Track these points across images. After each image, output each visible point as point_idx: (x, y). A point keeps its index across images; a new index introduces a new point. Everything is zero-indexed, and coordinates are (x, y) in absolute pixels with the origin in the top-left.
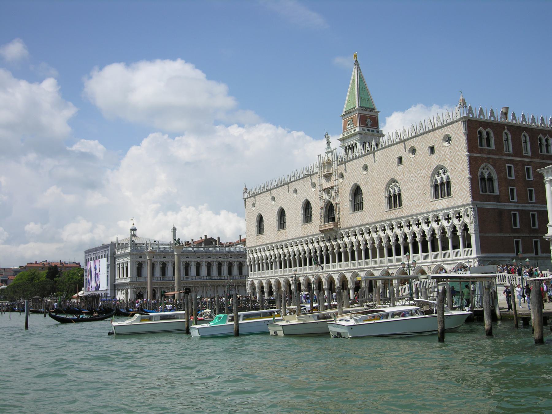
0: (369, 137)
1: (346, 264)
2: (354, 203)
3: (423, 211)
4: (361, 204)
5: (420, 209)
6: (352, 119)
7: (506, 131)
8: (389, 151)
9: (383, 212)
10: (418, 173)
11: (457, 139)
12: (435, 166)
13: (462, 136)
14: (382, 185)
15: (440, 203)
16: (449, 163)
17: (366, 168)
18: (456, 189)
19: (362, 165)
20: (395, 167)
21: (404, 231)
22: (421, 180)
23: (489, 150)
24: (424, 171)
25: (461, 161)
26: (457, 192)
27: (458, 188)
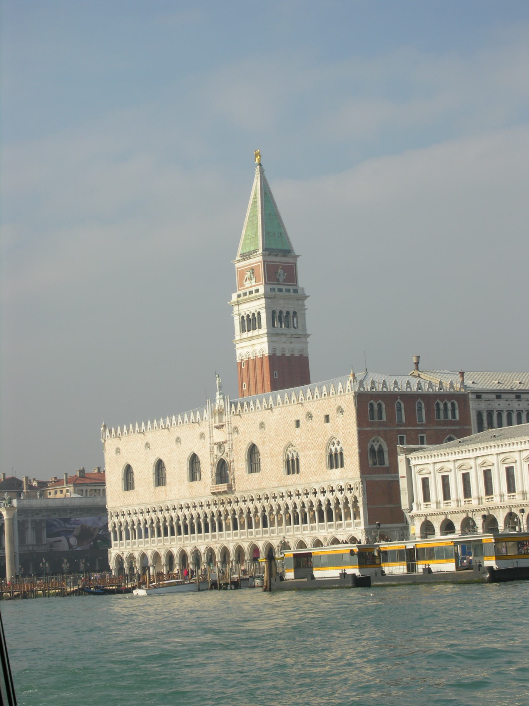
0: (282, 302)
1: (243, 532)
2: (251, 463)
3: (318, 480)
4: (259, 464)
5: (316, 478)
6: (253, 269)
7: (399, 400)
9: (281, 478)
10: (315, 440)
11: (348, 413)
12: (330, 437)
14: (280, 447)
15: (334, 473)
17: (262, 425)
23: (380, 422)
24: (320, 439)
25: (352, 435)
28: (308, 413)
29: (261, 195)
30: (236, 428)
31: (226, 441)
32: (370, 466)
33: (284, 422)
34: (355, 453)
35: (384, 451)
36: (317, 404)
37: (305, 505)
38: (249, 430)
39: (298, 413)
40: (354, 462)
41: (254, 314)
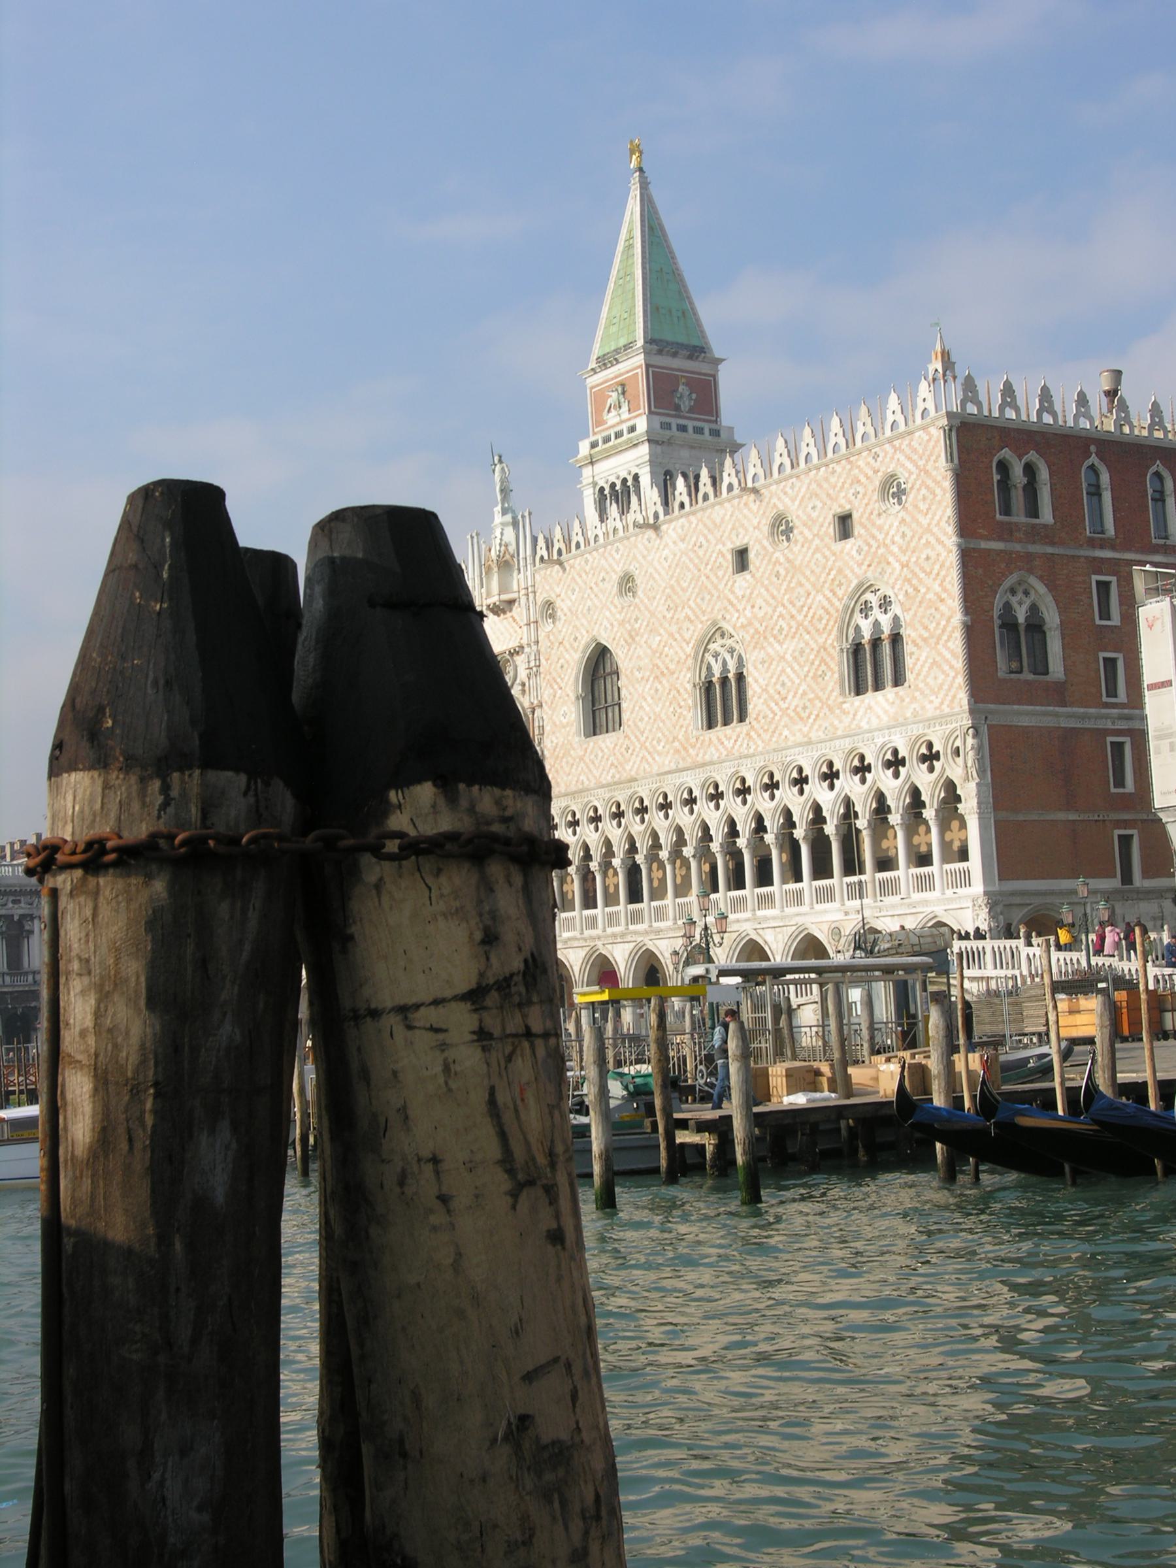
0: (685, 453)
2: (593, 705)
3: (814, 736)
4: (617, 708)
5: (805, 729)
6: (623, 385)
8: (705, 525)
9: (687, 740)
10: (799, 604)
11: (924, 491)
12: (855, 582)
13: (939, 478)
14: (684, 645)
15: (870, 708)
16: (897, 572)
17: (627, 584)
18: (919, 663)
19: (616, 573)
20: (724, 582)
21: (753, 804)
22: (810, 628)
23: (1034, 526)
24: (820, 597)
25: (937, 567)
26: (924, 673)
27: (927, 658)
28: (776, 520)
29: (643, 231)
30: (549, 604)
31: (522, 647)
32: (1001, 674)
33: (696, 561)
34: (949, 629)
35: (1045, 628)
36: (810, 484)
37: (767, 823)
38: (589, 603)
39: (742, 525)
40: (947, 661)
41: (625, 481)
